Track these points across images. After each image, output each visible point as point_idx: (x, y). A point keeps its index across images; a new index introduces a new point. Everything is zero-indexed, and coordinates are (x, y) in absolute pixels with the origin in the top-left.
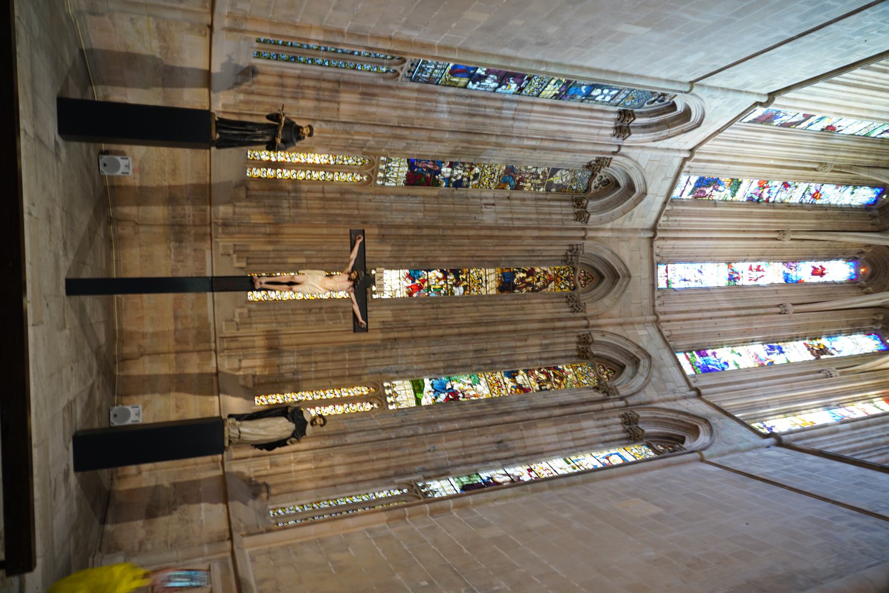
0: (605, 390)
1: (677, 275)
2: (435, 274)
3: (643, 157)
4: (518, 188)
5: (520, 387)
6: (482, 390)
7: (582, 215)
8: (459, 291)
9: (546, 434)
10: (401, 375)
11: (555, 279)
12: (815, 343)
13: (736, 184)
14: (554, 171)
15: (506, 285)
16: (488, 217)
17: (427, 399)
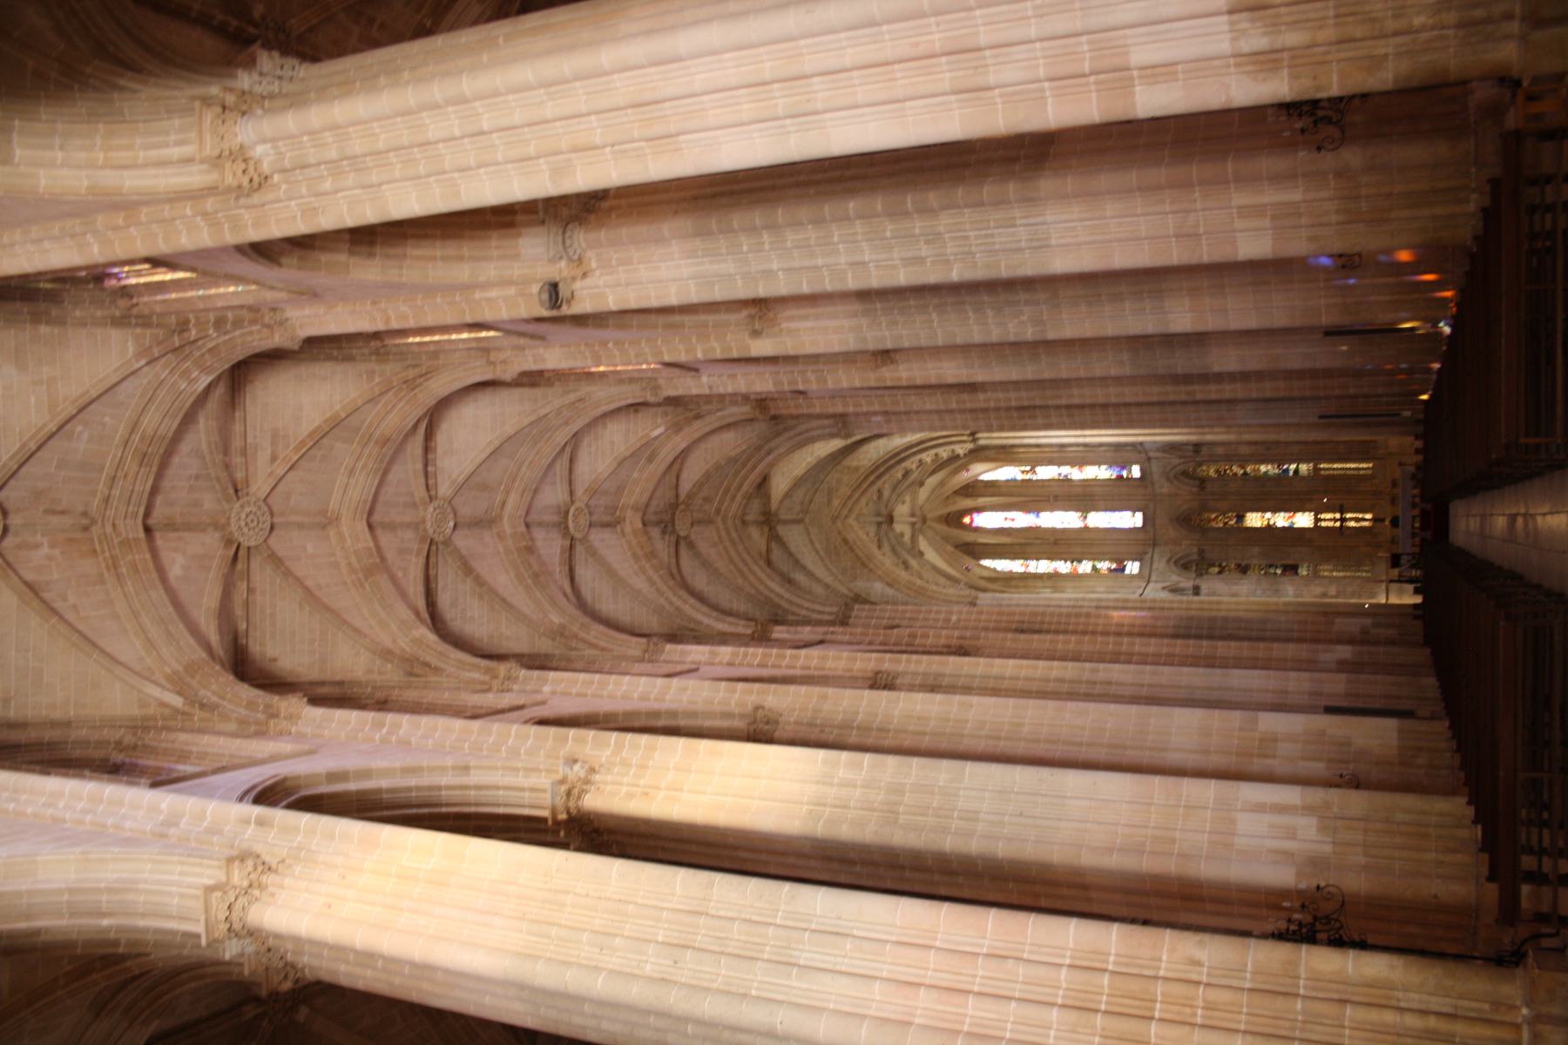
0: (1200, 464)
1: (1130, 520)
2: (1280, 524)
3: (1175, 578)
4: (1239, 566)
5: (1242, 467)
6: (1263, 468)
7: (1201, 552)
8: (1268, 515)
9: (1244, 450)
10: (1304, 478)
11: (1210, 520)
12: (1027, 477)
13: (1094, 568)
14: (1220, 573)
15: (1241, 518)
16: (1256, 550)
17: (1293, 467)
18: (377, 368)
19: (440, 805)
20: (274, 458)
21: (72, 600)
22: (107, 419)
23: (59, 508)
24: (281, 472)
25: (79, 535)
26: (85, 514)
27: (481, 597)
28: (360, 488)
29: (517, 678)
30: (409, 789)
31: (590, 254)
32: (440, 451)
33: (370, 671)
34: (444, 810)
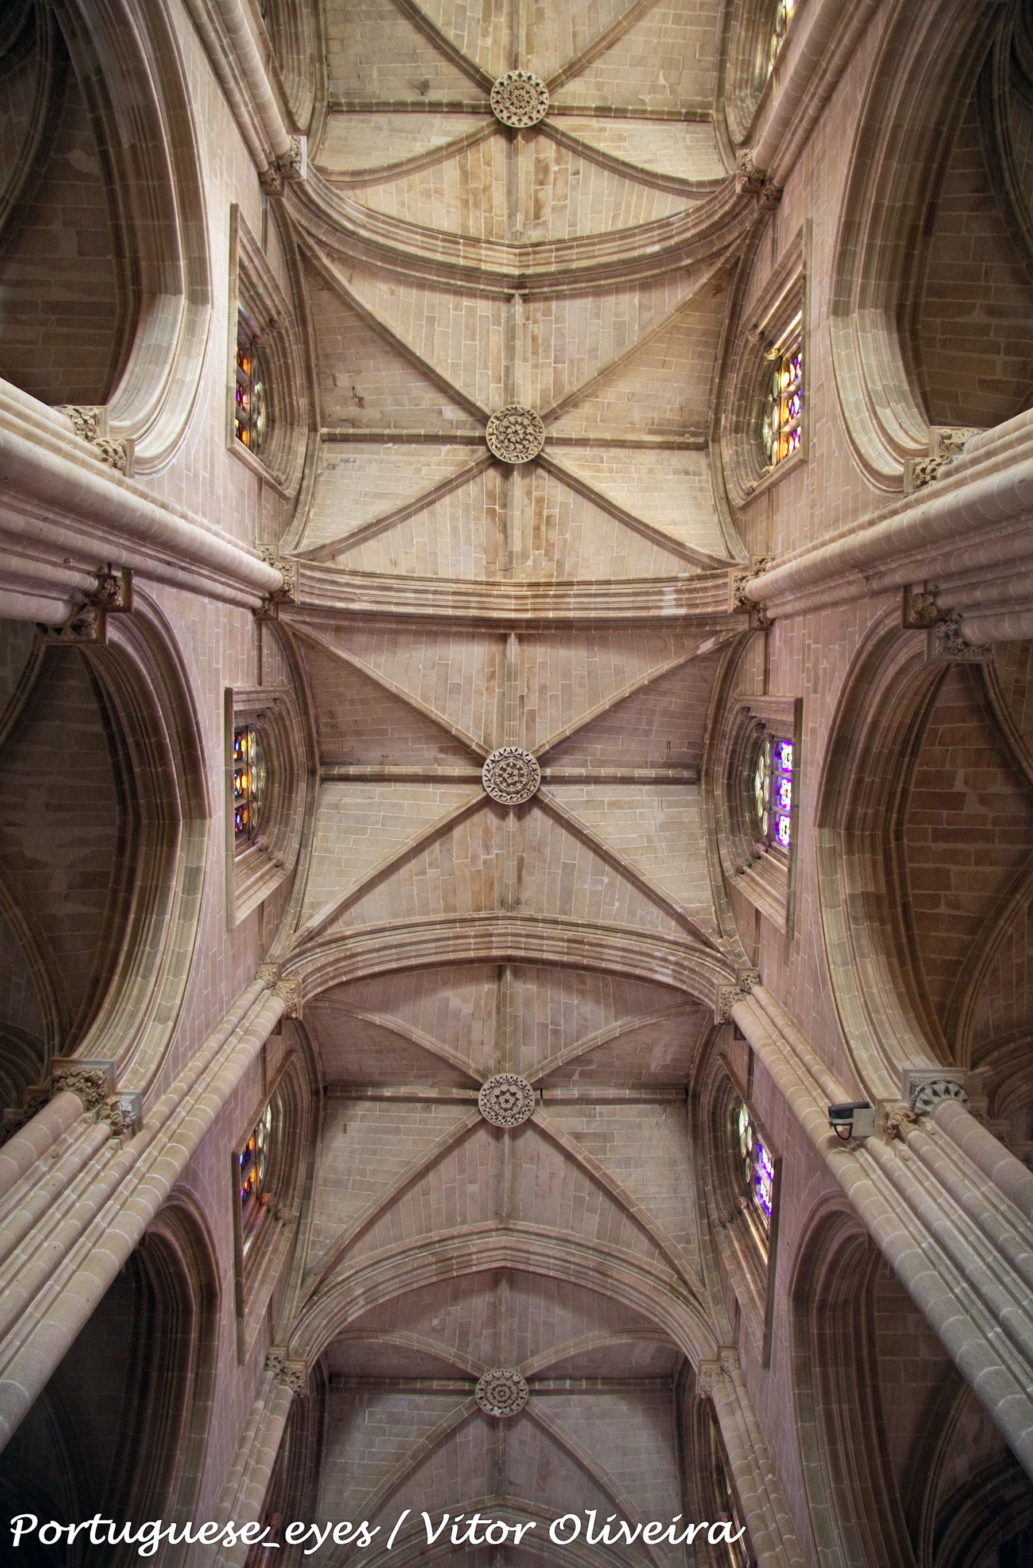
18: (694, 1245)
19: (124, 976)
20: (578, 1136)
21: (430, 872)
22: (617, 905)
23: (524, 872)
24: (563, 1141)
25: (496, 895)
26: (518, 902)
27: (400, 1457)
28: (544, 1256)
29: (283, 1382)
30: (155, 945)
31: (929, 1124)
32: (591, 1399)
33: (318, 1232)
34: (116, 978)
